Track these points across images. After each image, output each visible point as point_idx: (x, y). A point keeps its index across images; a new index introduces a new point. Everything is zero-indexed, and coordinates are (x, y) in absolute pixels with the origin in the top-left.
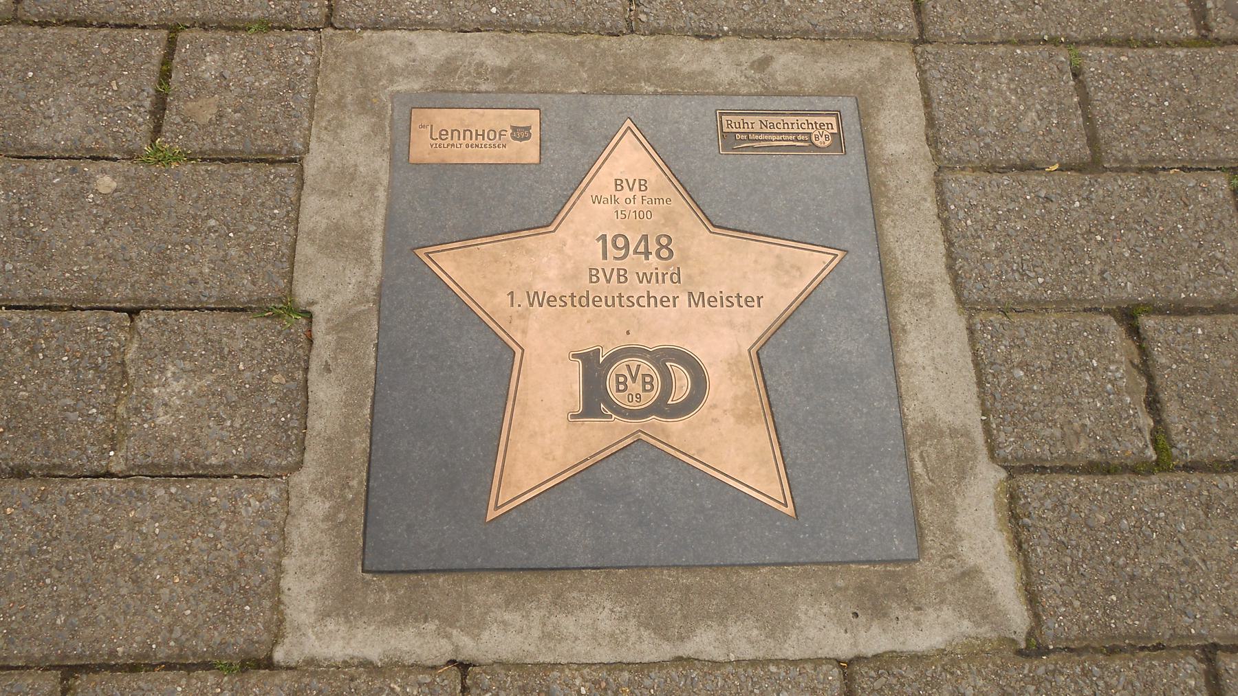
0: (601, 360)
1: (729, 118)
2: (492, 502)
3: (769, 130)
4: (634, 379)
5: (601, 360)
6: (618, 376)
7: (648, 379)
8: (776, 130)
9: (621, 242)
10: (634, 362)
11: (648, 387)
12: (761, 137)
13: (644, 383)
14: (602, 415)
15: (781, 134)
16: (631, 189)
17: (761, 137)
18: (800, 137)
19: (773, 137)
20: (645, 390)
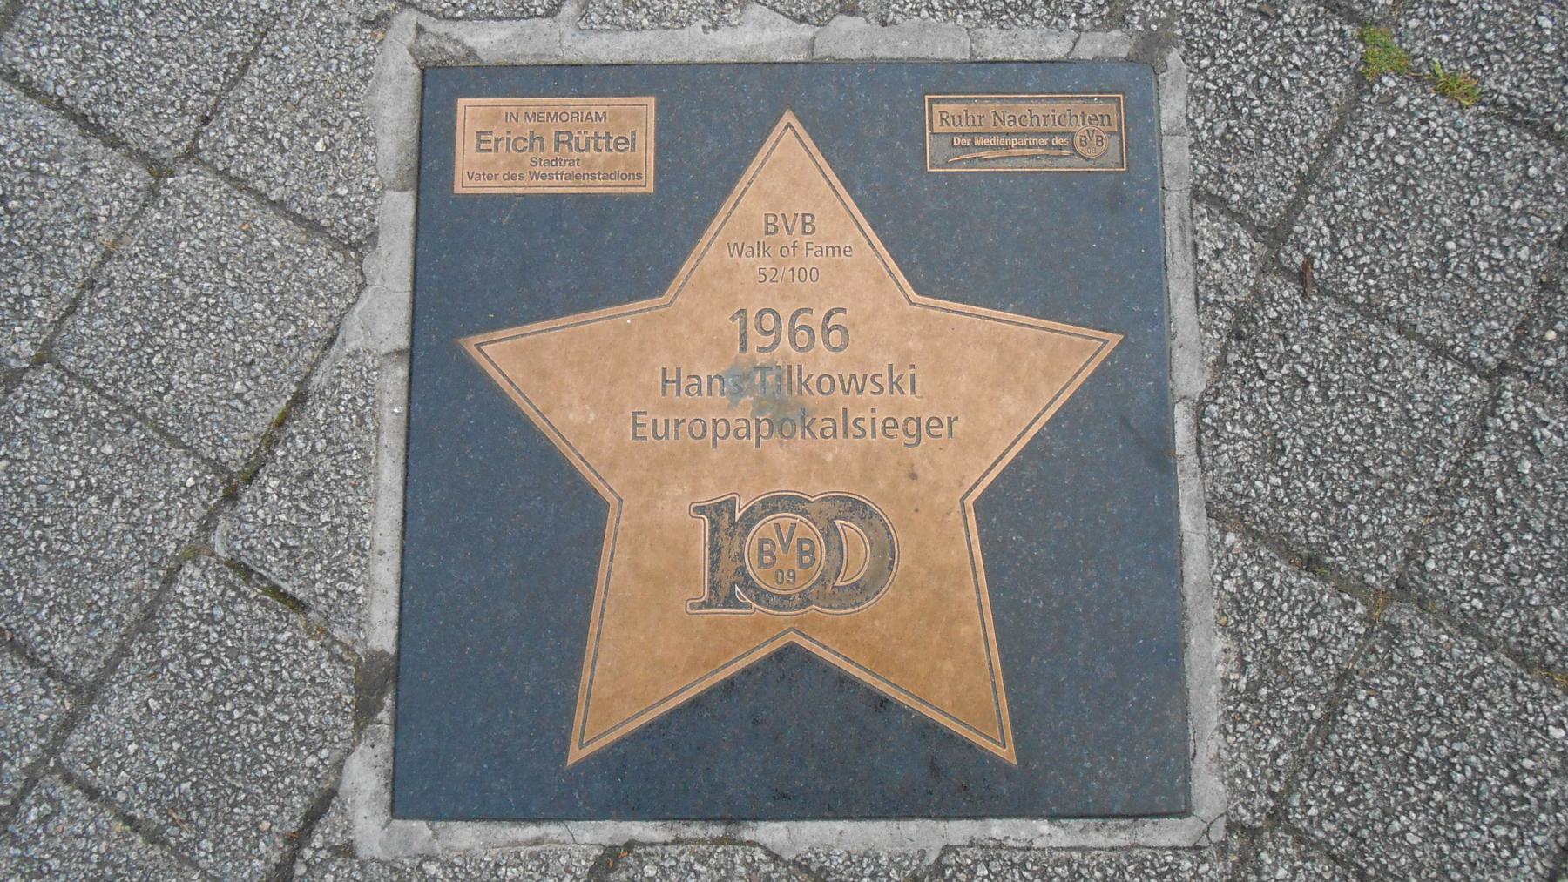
0: (738, 515)
1: (942, 107)
2: (574, 745)
3: (1007, 128)
4: (785, 546)
5: (738, 515)
6: (762, 541)
7: (806, 547)
8: (1019, 128)
9: (769, 322)
10: (787, 518)
11: (807, 559)
12: (994, 141)
13: (802, 553)
14: (738, 605)
15: (1028, 134)
16: (789, 232)
17: (994, 141)
18: (1056, 141)
19: (1013, 142)
20: (801, 565)
